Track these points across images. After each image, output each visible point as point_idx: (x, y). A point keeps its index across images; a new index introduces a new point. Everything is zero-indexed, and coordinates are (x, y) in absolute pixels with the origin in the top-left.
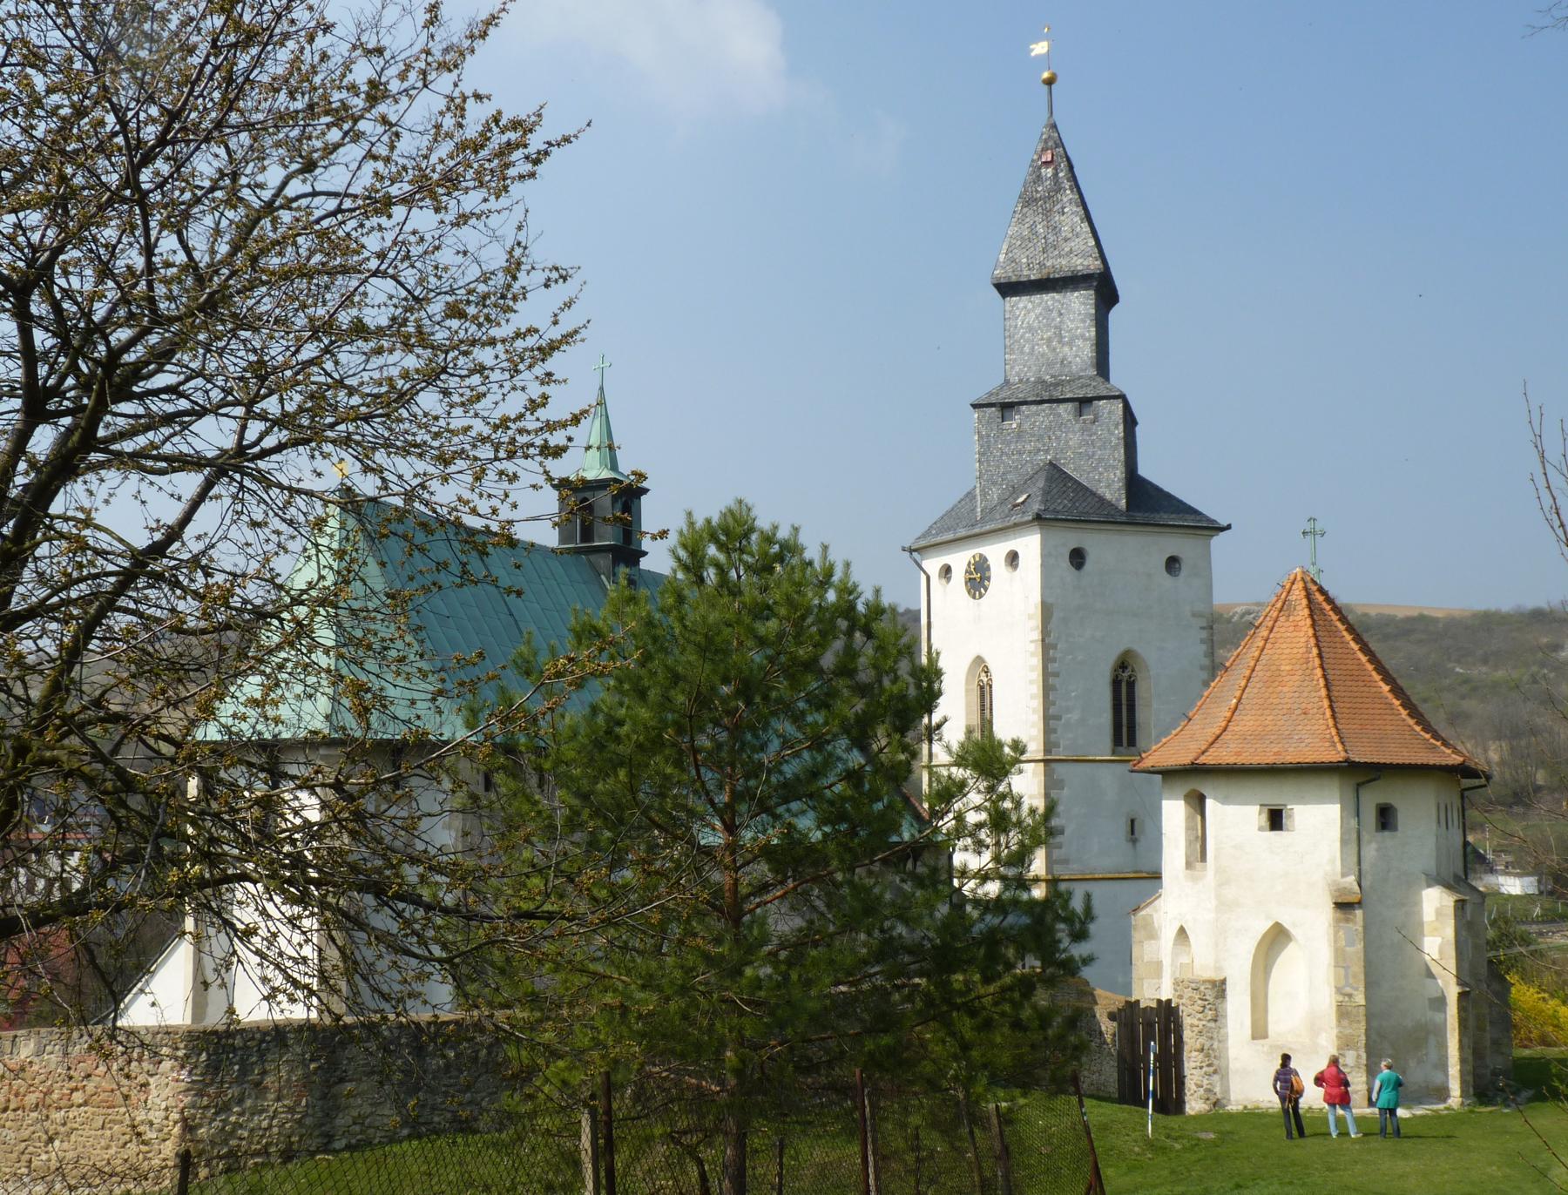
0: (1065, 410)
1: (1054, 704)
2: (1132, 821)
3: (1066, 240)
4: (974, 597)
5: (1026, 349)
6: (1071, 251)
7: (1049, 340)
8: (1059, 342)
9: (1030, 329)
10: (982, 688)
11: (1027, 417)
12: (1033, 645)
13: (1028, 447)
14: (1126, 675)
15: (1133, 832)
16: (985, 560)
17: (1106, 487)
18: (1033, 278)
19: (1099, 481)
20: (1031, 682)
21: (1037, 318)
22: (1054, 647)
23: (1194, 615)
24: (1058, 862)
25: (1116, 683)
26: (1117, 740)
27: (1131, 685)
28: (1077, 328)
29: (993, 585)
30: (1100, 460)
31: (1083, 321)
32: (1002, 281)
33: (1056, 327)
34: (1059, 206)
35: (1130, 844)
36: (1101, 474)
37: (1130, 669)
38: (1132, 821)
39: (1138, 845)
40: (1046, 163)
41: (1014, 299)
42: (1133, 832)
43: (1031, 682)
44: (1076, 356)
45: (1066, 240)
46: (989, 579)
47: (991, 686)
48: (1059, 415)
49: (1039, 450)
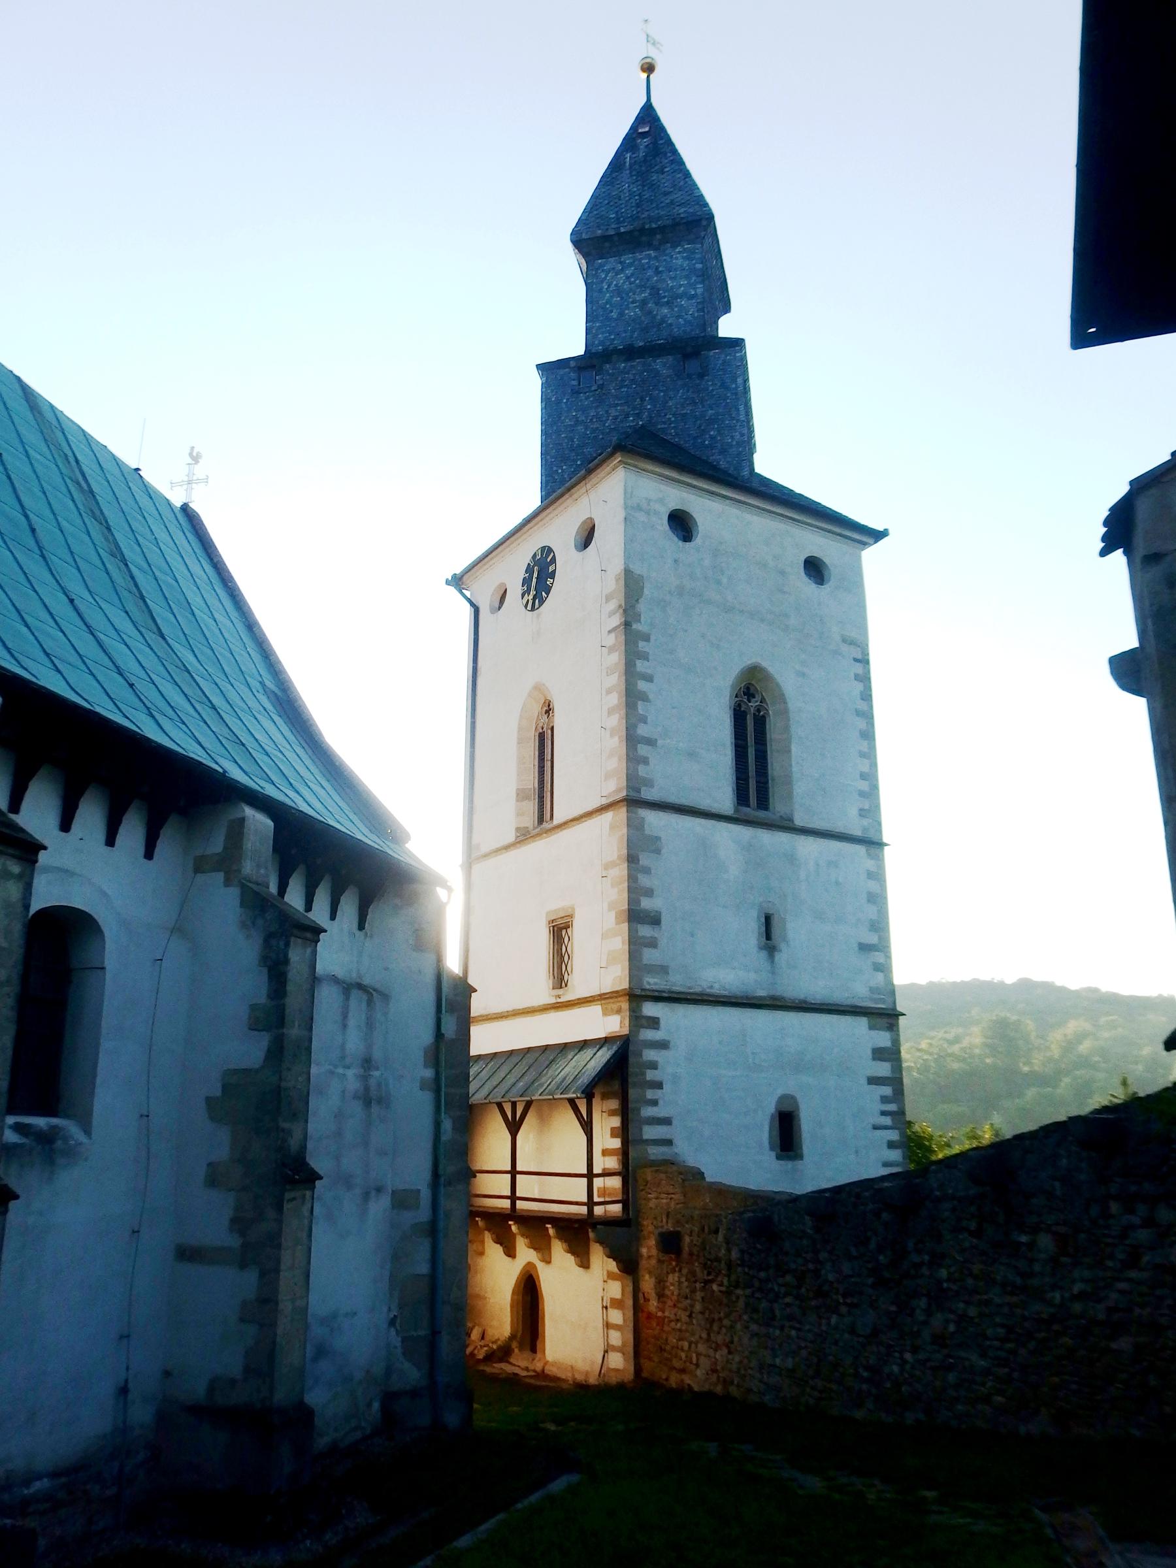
0: (662, 365)
1: (644, 720)
2: (768, 920)
3: (666, 194)
4: (533, 609)
5: (614, 315)
6: (672, 202)
7: (644, 302)
8: (656, 304)
9: (619, 291)
10: (542, 737)
11: (613, 374)
12: (613, 635)
13: (613, 412)
14: (753, 704)
15: (768, 936)
16: (550, 550)
17: (721, 453)
18: (622, 230)
19: (711, 447)
20: (609, 692)
21: (628, 278)
22: (647, 638)
23: (844, 641)
24: (652, 969)
25: (738, 716)
26: (742, 796)
27: (761, 722)
28: (681, 286)
29: (559, 585)
30: (712, 421)
31: (687, 277)
32: (584, 236)
33: (653, 288)
34: (657, 168)
35: (764, 954)
36: (712, 438)
37: (758, 698)
38: (768, 920)
39: (777, 956)
40: (644, 135)
41: (600, 261)
42: (768, 936)
43: (609, 692)
44: (679, 317)
45: (666, 194)
46: (552, 575)
47: (552, 729)
48: (657, 373)
49: (627, 416)
